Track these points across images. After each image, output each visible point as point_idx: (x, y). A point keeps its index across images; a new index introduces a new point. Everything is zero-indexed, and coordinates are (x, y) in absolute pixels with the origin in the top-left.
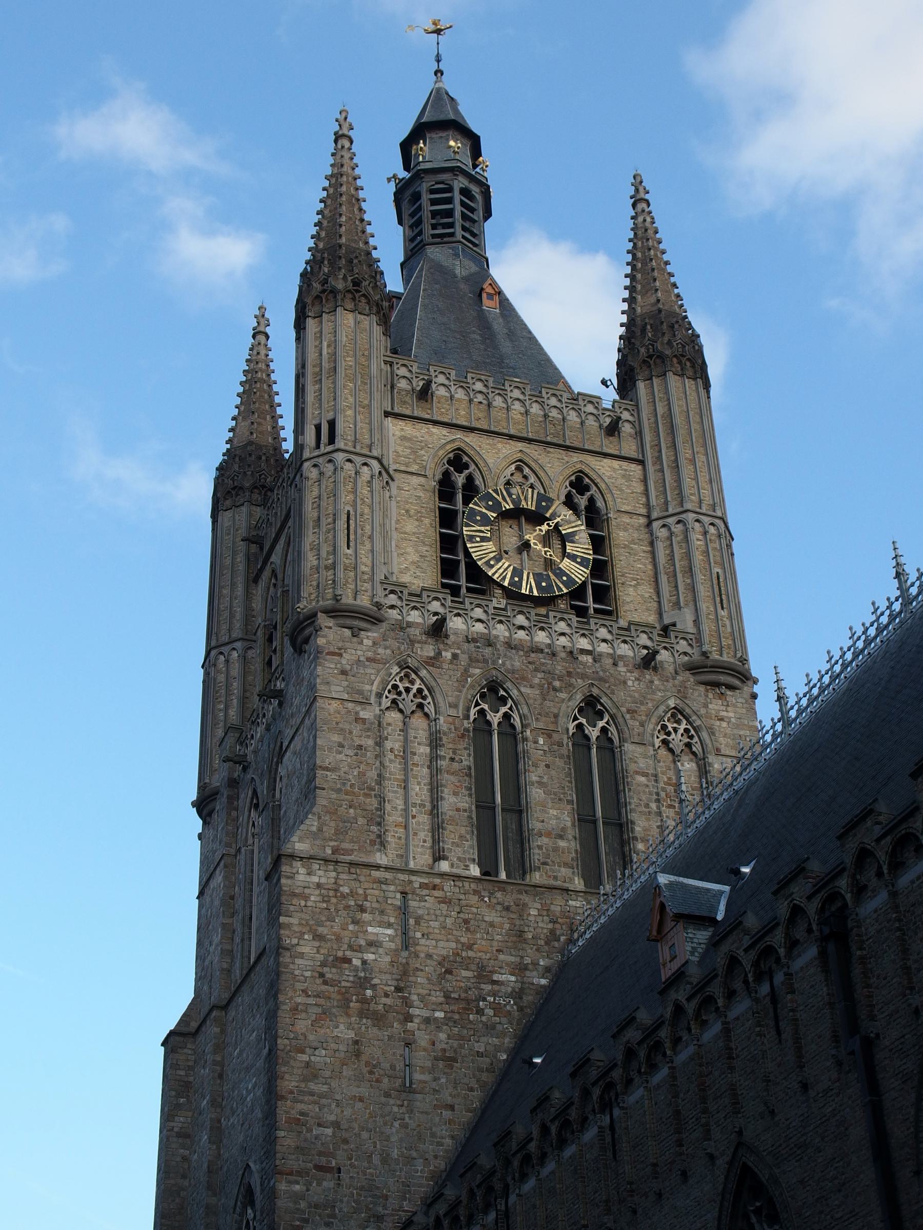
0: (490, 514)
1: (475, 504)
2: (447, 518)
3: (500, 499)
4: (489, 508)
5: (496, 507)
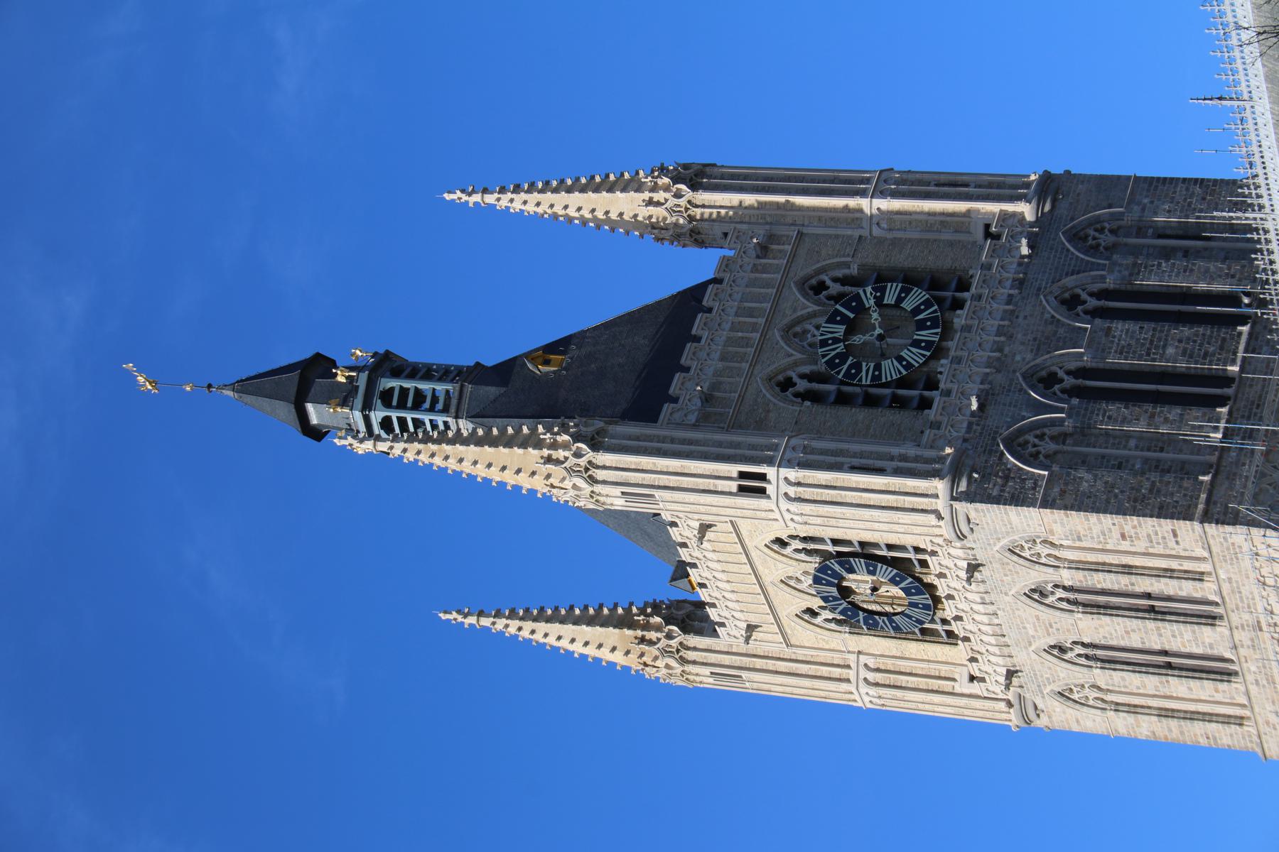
0: (849, 362)
2: (843, 400)
3: (833, 353)
5: (843, 357)
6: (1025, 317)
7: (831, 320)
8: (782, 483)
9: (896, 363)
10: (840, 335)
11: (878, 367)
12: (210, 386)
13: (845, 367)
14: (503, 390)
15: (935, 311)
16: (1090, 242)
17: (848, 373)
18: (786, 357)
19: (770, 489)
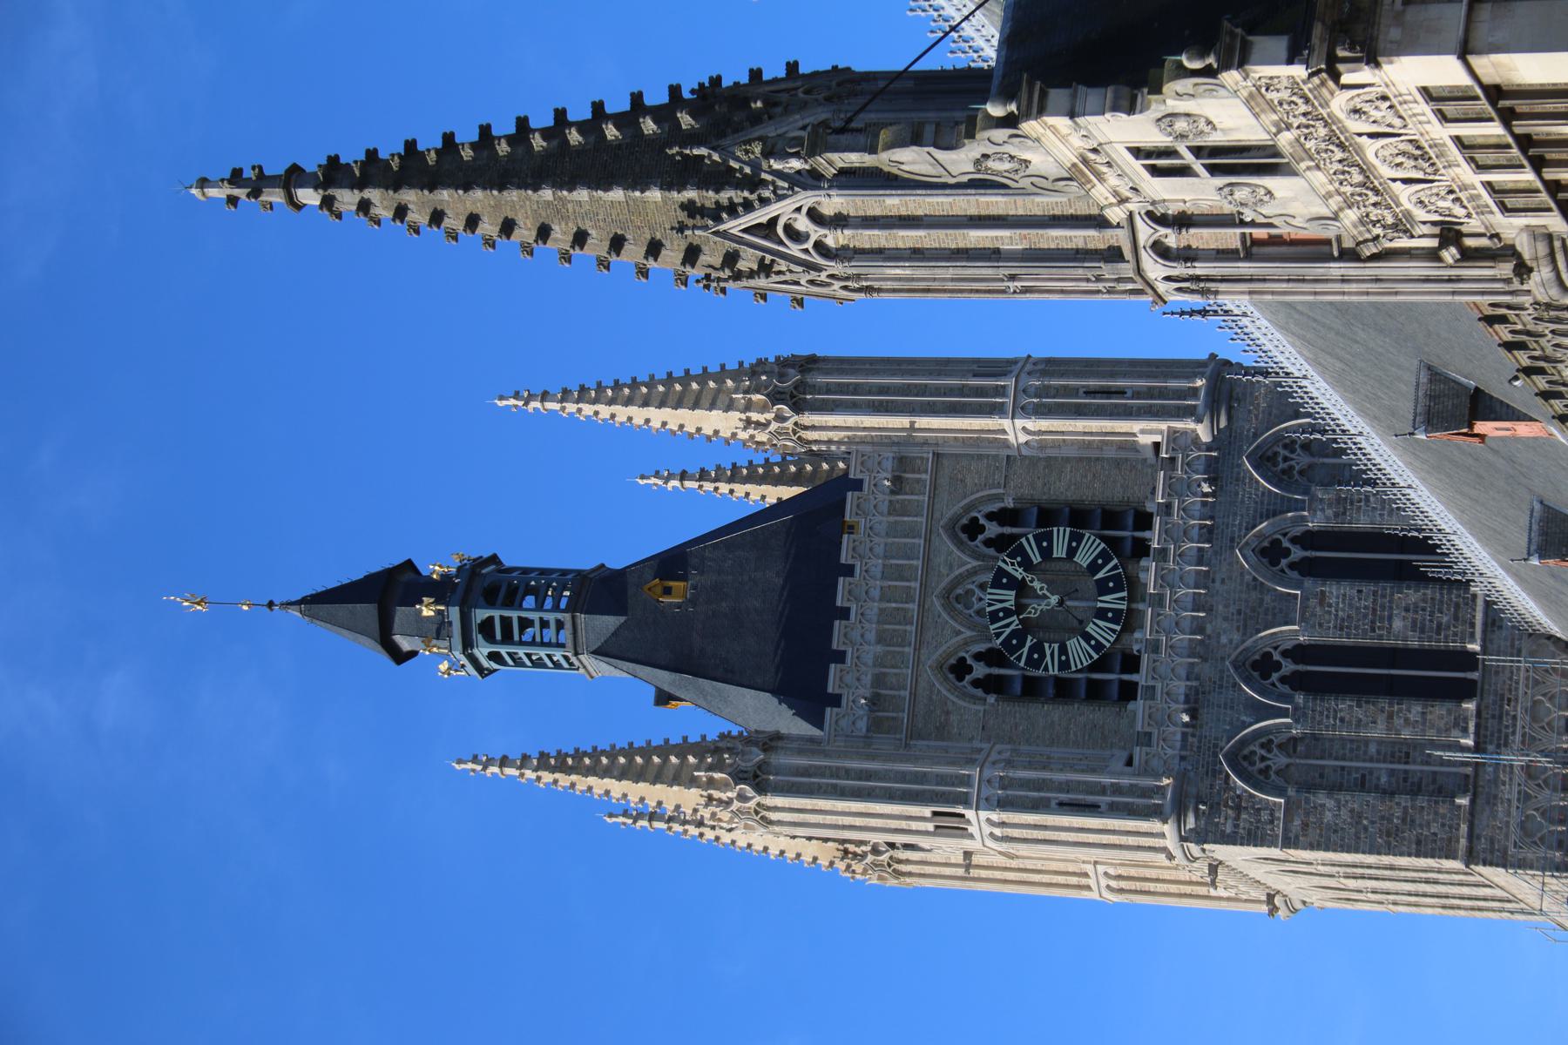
0: (1028, 644)
1: (1019, 658)
2: (1032, 689)
3: (1008, 631)
4: (1022, 644)
5: (1020, 635)
6: (1223, 581)
7: (996, 584)
8: (983, 825)
9: (1083, 643)
10: (1010, 604)
11: (1063, 650)
12: (271, 604)
13: (1026, 650)
14: (622, 619)
15: (1115, 567)
16: (1282, 466)
17: (1030, 662)
18: (955, 637)
19: (972, 829)
